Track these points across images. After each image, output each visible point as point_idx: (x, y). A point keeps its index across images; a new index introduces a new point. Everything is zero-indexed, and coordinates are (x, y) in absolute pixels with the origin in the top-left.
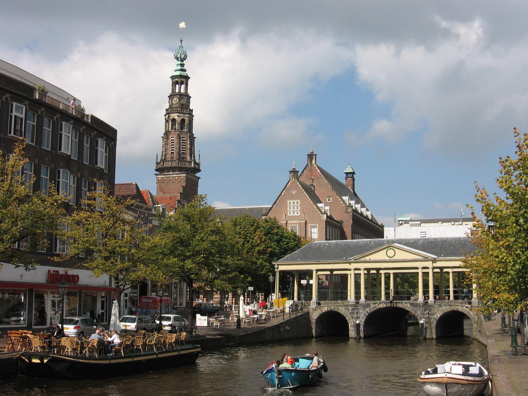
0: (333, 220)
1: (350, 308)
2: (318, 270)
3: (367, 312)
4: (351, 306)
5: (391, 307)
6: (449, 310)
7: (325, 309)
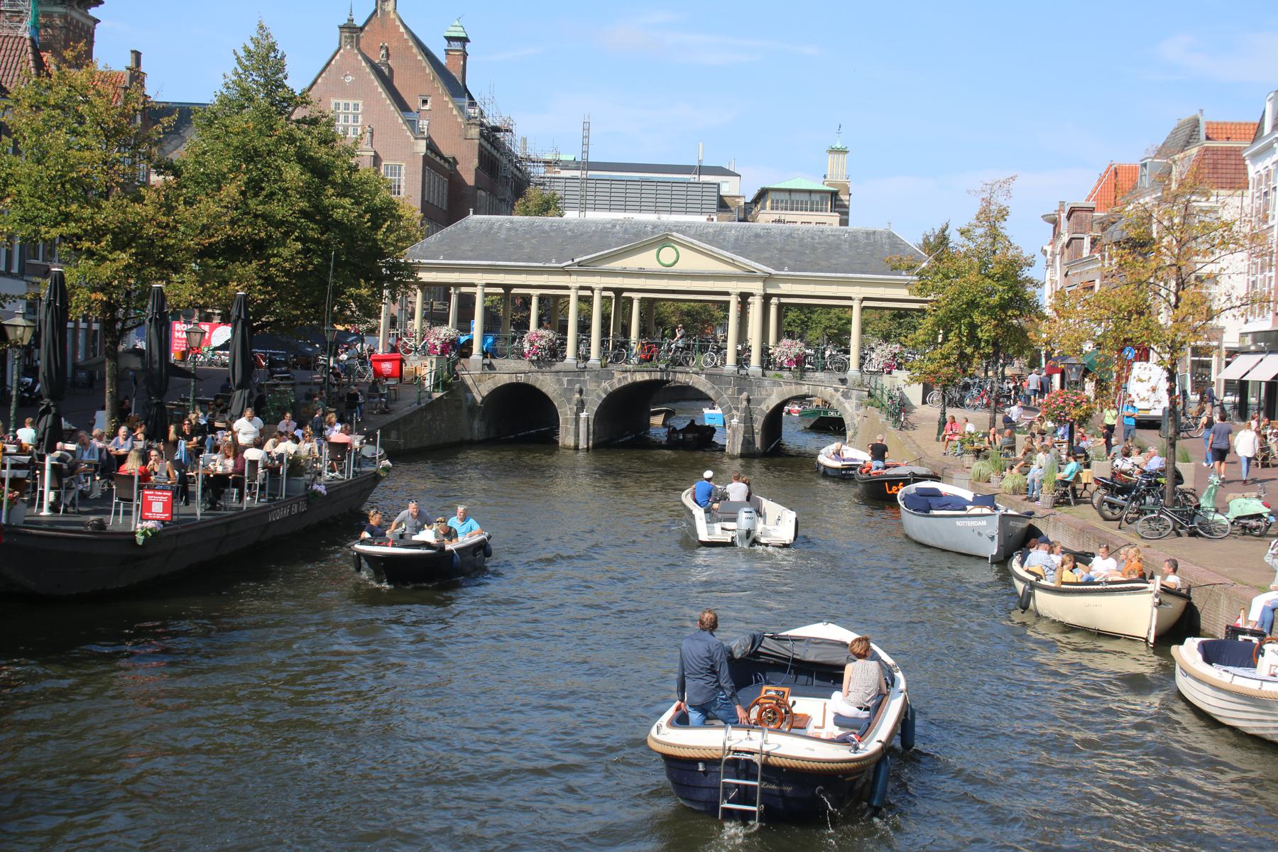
0: (438, 154)
1: (565, 380)
2: (488, 285)
3: (605, 390)
4: (566, 372)
7: (504, 379)
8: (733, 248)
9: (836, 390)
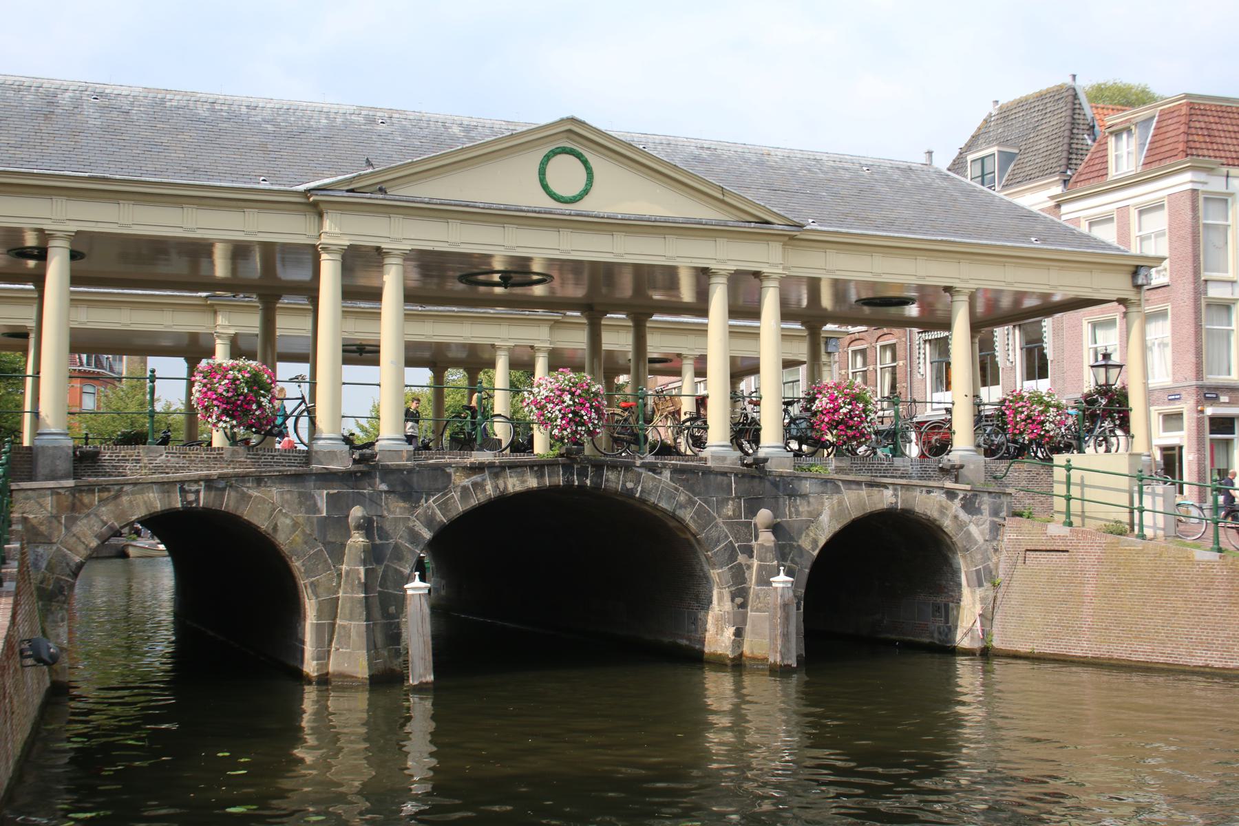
5: (569, 486)
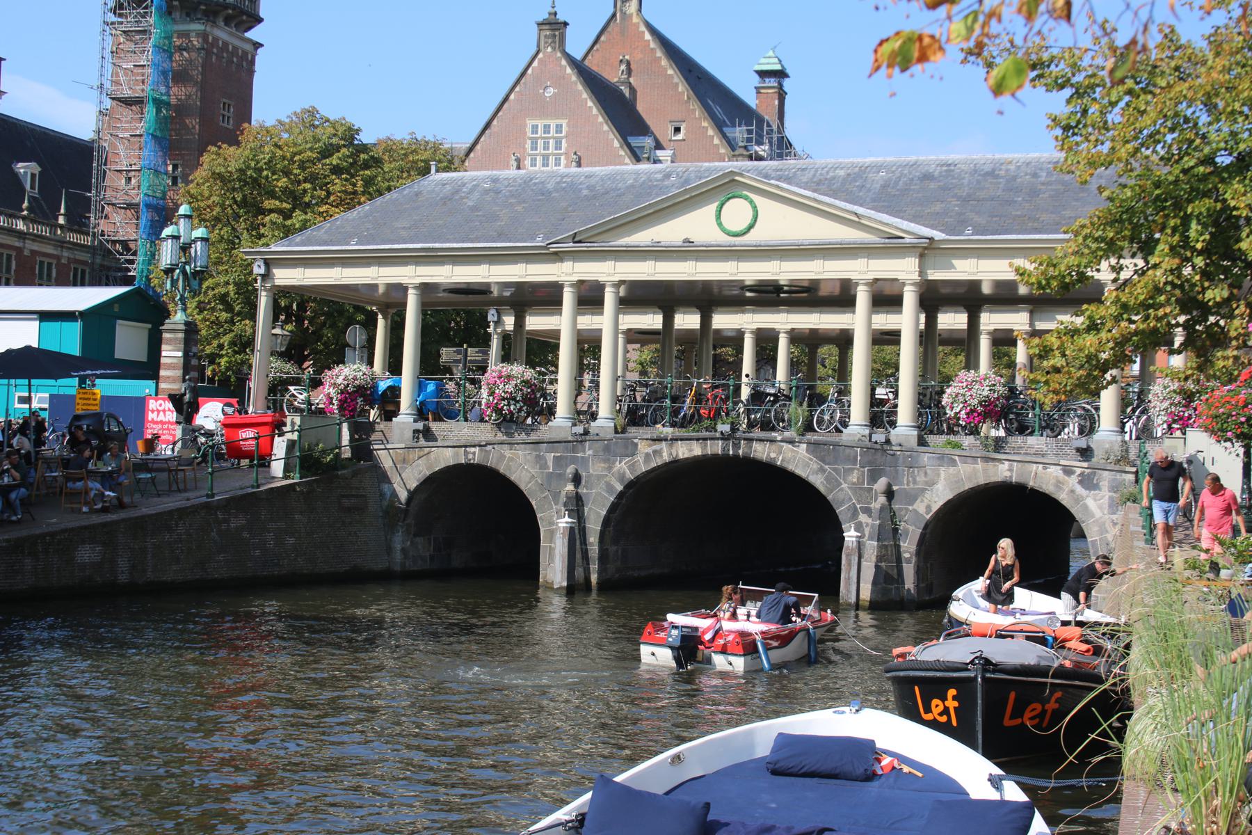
1: (550, 457)
3: (621, 477)
6: (982, 481)
7: (444, 457)
8: (874, 200)
9: (1068, 471)
